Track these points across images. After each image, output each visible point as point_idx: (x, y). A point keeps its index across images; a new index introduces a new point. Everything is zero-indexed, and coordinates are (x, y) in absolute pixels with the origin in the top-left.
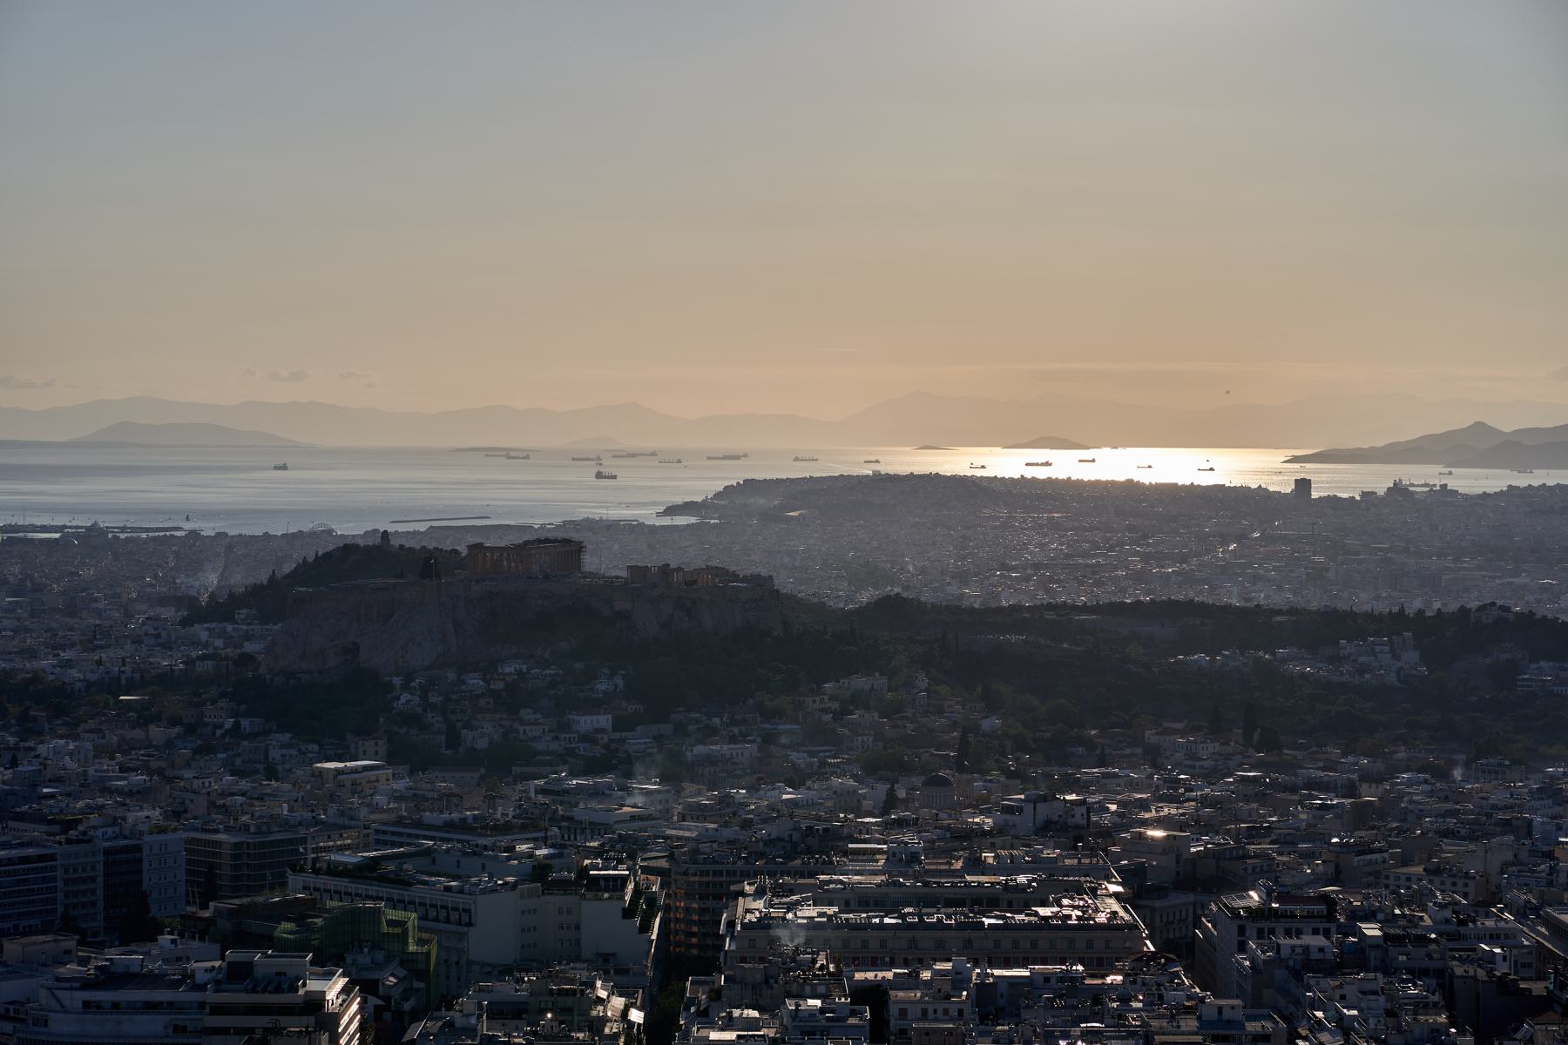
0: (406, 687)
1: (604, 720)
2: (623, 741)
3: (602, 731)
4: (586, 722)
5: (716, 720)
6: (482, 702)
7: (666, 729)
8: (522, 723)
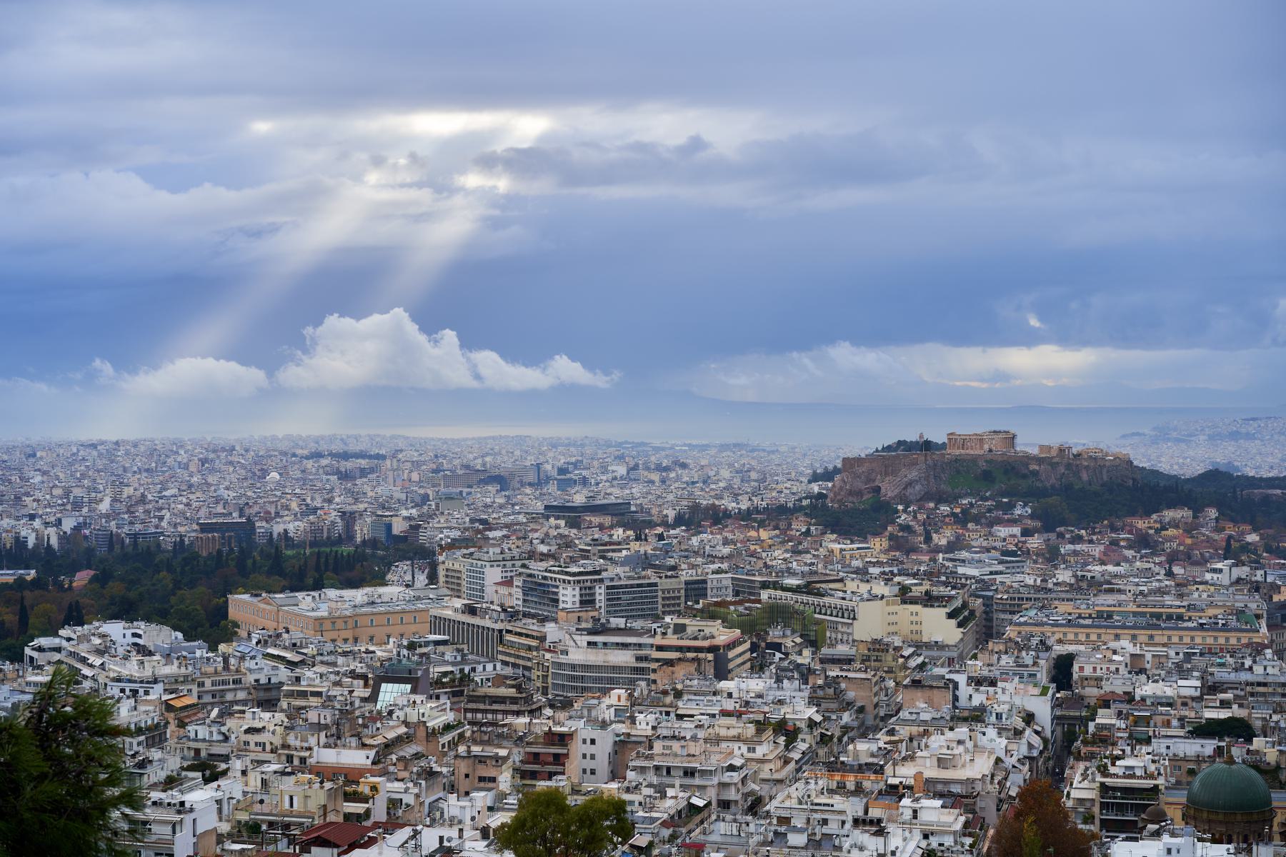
0: (905, 511)
1: (1016, 530)
2: (1025, 542)
3: (1014, 536)
4: (1002, 531)
5: (1083, 532)
6: (947, 520)
7: (1053, 536)
8: (968, 530)
